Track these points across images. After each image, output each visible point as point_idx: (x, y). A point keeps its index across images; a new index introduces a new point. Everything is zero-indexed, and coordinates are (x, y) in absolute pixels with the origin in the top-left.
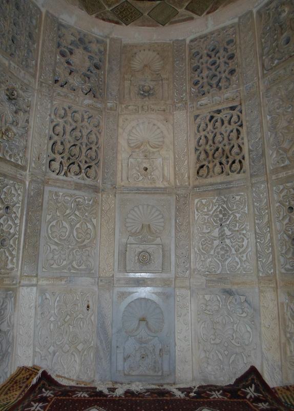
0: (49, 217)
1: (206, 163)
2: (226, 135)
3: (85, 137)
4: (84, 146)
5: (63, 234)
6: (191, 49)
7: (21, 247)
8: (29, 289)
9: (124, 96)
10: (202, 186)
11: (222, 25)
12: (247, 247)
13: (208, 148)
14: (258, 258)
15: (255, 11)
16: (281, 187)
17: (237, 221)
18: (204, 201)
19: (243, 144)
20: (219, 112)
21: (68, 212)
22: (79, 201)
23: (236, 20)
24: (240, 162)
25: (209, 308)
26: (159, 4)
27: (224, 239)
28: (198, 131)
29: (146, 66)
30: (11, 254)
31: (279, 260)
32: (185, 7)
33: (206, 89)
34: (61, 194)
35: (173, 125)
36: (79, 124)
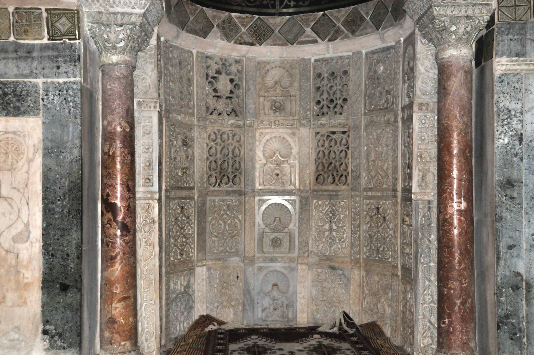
0: (210, 218)
1: (322, 173)
2: (338, 153)
3: (231, 152)
4: (230, 160)
5: (220, 229)
6: (314, 69)
7: (196, 242)
8: (202, 268)
9: (259, 112)
10: (320, 191)
11: (340, 54)
12: (346, 238)
13: (324, 161)
14: (351, 247)
15: (364, 52)
16: (368, 201)
17: (340, 220)
18: (320, 202)
19: (348, 163)
20: (334, 133)
21: (222, 212)
22: (229, 204)
23: (351, 54)
24: (346, 176)
25: (320, 278)
26: (289, 19)
27: (332, 232)
28: (318, 146)
29: (276, 83)
30: (191, 248)
31: (363, 250)
32: (311, 27)
33: (325, 110)
34: (217, 200)
35: (299, 139)
36: (226, 142)
